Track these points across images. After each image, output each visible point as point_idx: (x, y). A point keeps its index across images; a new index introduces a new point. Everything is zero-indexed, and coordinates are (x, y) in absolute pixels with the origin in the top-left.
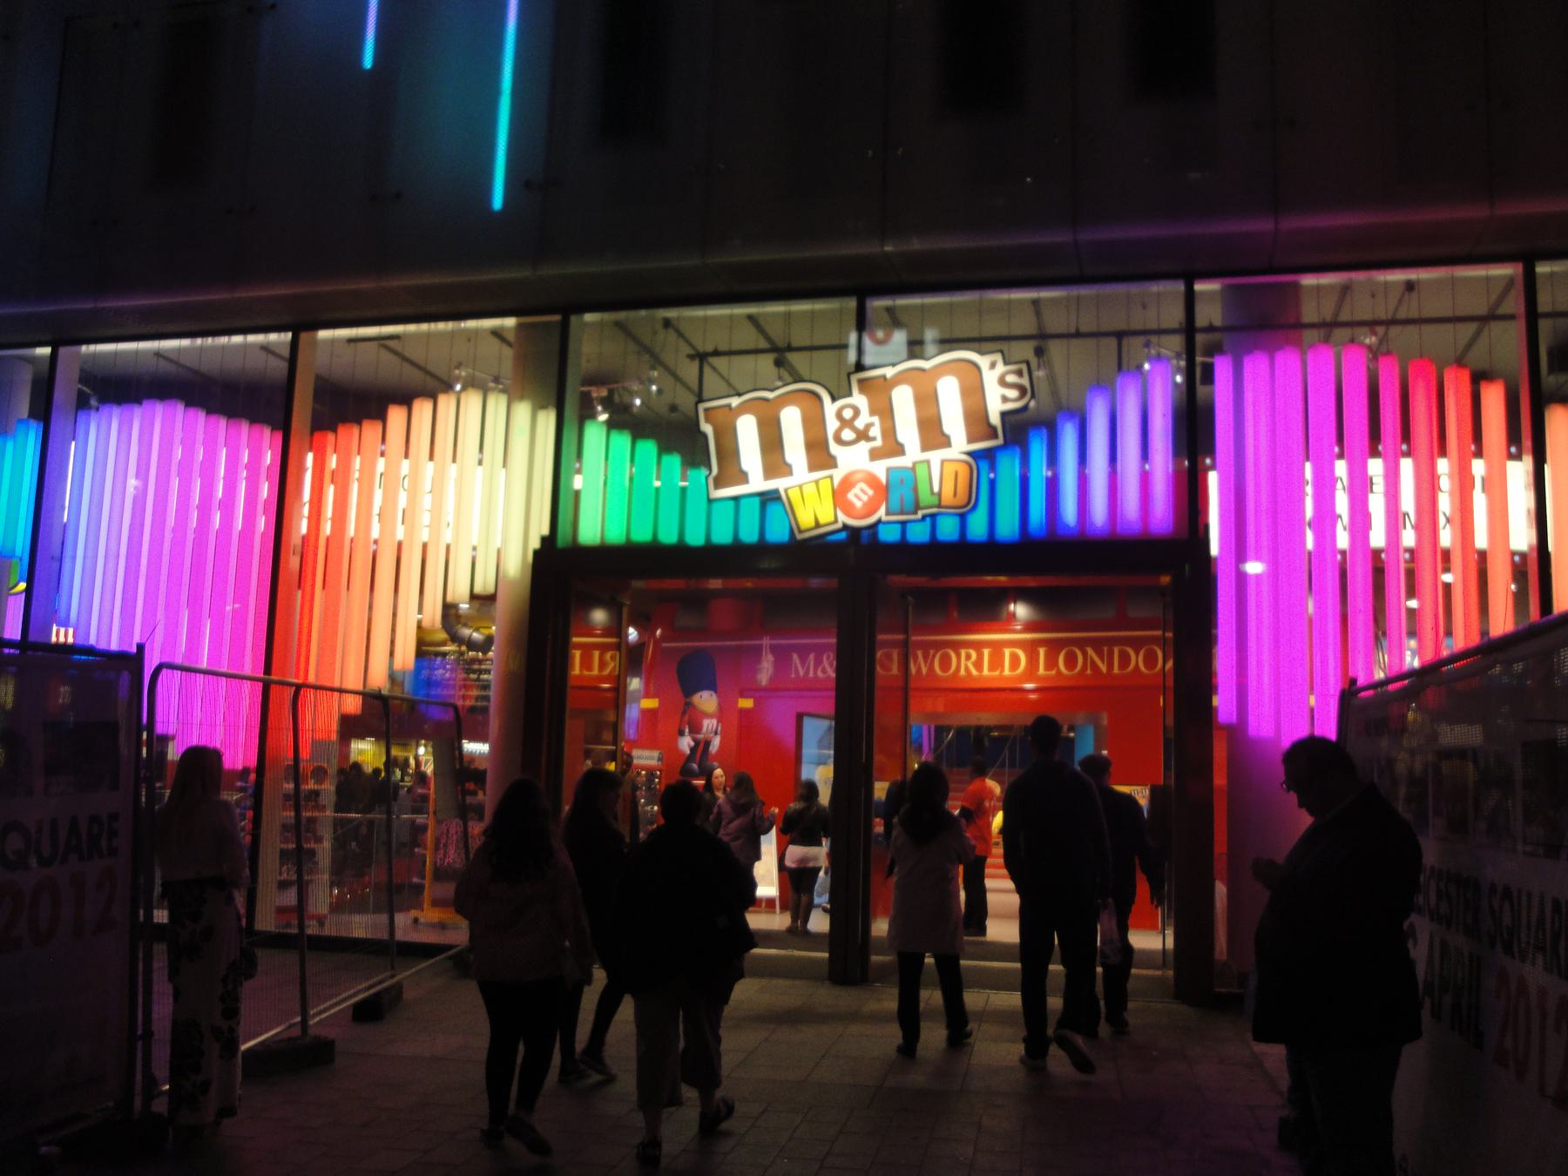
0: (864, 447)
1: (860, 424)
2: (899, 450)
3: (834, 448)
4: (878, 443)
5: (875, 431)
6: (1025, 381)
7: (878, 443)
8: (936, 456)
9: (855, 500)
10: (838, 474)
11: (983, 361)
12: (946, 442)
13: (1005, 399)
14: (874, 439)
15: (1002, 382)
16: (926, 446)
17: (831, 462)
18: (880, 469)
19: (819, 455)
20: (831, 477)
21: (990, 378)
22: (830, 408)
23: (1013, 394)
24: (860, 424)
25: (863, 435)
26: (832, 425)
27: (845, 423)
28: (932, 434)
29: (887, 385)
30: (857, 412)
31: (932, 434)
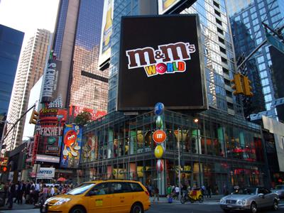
2: (169, 60)
6: (194, 48)
8: (177, 61)
11: (185, 44)
12: (179, 59)
15: (189, 47)
16: (174, 59)
17: (155, 62)
18: (165, 63)
19: (152, 61)
21: (187, 47)
22: (154, 52)
25: (161, 57)
26: (155, 55)
27: (157, 55)
28: (176, 57)
29: (166, 48)
30: (160, 53)
31: (176, 57)
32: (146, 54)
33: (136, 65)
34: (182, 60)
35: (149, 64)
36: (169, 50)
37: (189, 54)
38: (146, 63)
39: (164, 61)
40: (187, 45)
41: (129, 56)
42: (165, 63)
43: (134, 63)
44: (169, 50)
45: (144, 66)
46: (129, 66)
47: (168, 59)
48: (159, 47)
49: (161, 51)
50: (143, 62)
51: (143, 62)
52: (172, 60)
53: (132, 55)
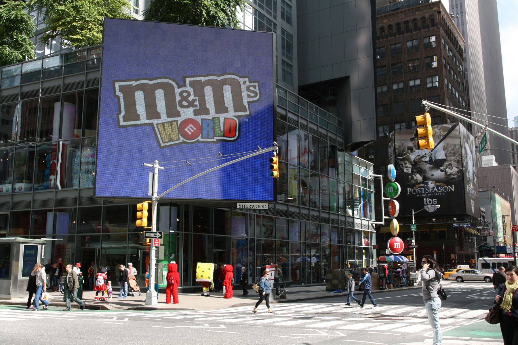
0: (191, 110)
1: (190, 99)
2: (207, 112)
3: (179, 109)
4: (198, 108)
5: (197, 103)
6: (257, 90)
7: (198, 108)
8: (222, 116)
9: (188, 132)
10: (180, 120)
11: (241, 80)
12: (226, 111)
13: (249, 96)
14: (196, 106)
15: (248, 89)
17: (178, 115)
18: (199, 119)
19: (172, 112)
20: (177, 121)
22: (178, 91)
23: (252, 94)
24: (190, 99)
25: (191, 104)
26: (178, 98)
28: (221, 107)
31: (221, 107)
32: (160, 95)
33: (137, 117)
34: (231, 114)
35: (164, 118)
36: (208, 91)
37: (245, 103)
38: (157, 116)
39: (196, 113)
40: (244, 83)
41: (121, 95)
42: (199, 119)
43: (132, 113)
44: (208, 91)
45: (155, 122)
46: (121, 119)
47: (203, 110)
48: (188, 80)
49: (191, 90)
50: (152, 111)
51: (152, 111)
52: (213, 113)
53: (129, 93)
